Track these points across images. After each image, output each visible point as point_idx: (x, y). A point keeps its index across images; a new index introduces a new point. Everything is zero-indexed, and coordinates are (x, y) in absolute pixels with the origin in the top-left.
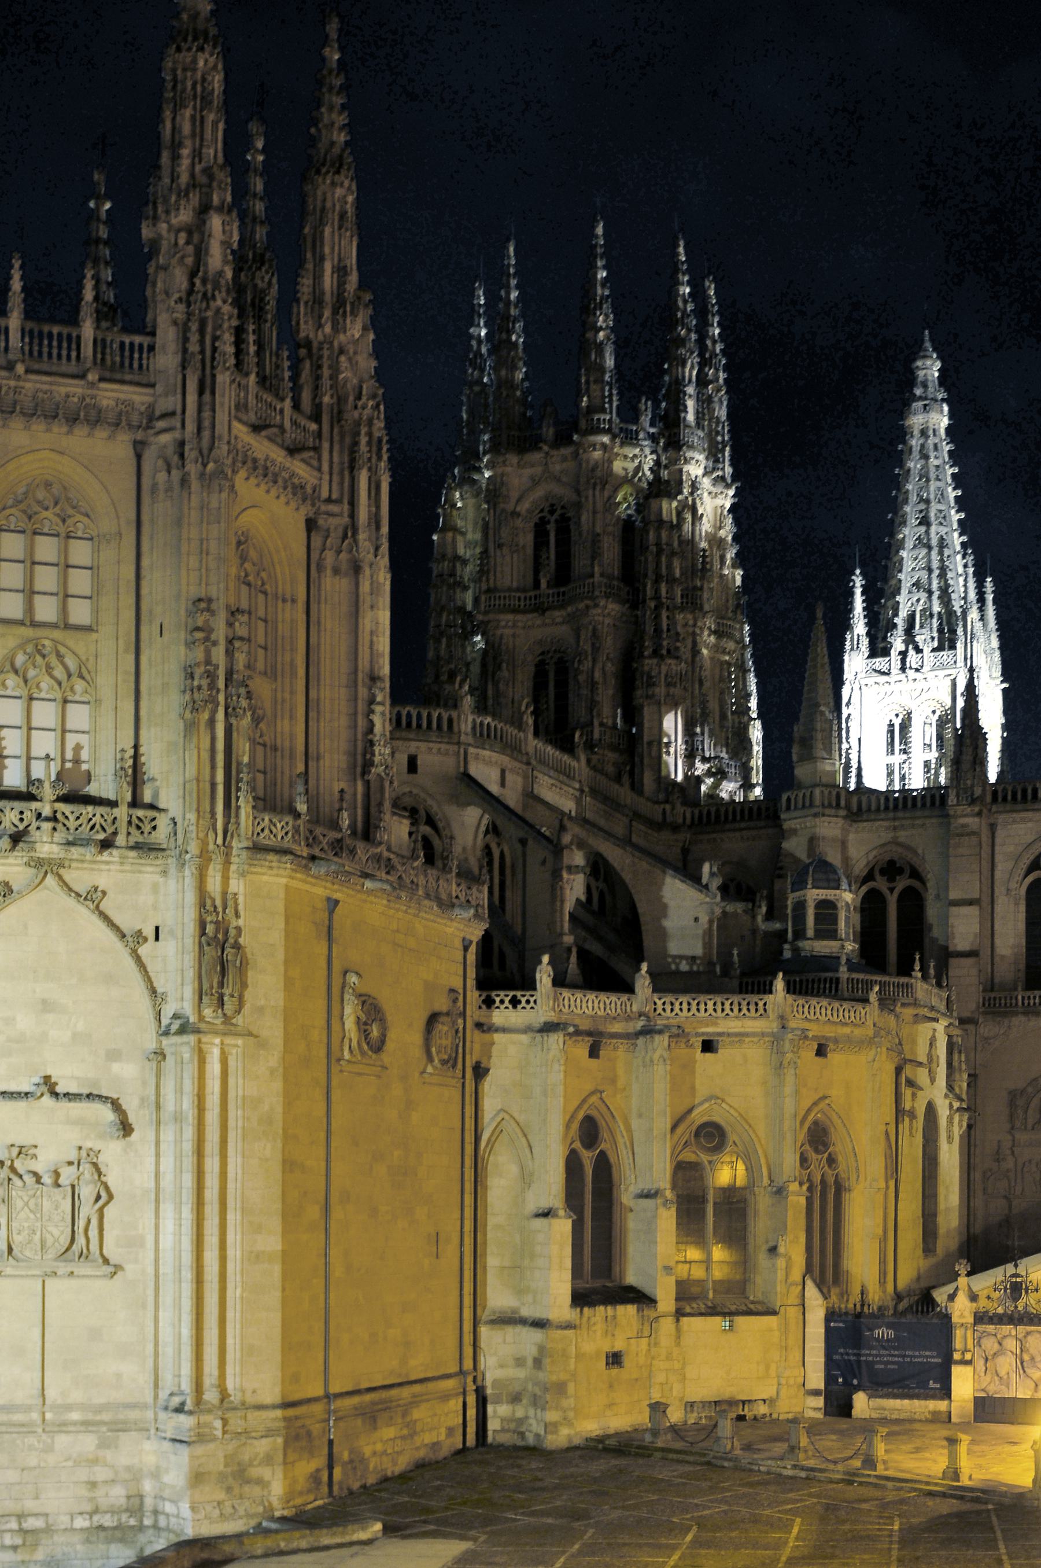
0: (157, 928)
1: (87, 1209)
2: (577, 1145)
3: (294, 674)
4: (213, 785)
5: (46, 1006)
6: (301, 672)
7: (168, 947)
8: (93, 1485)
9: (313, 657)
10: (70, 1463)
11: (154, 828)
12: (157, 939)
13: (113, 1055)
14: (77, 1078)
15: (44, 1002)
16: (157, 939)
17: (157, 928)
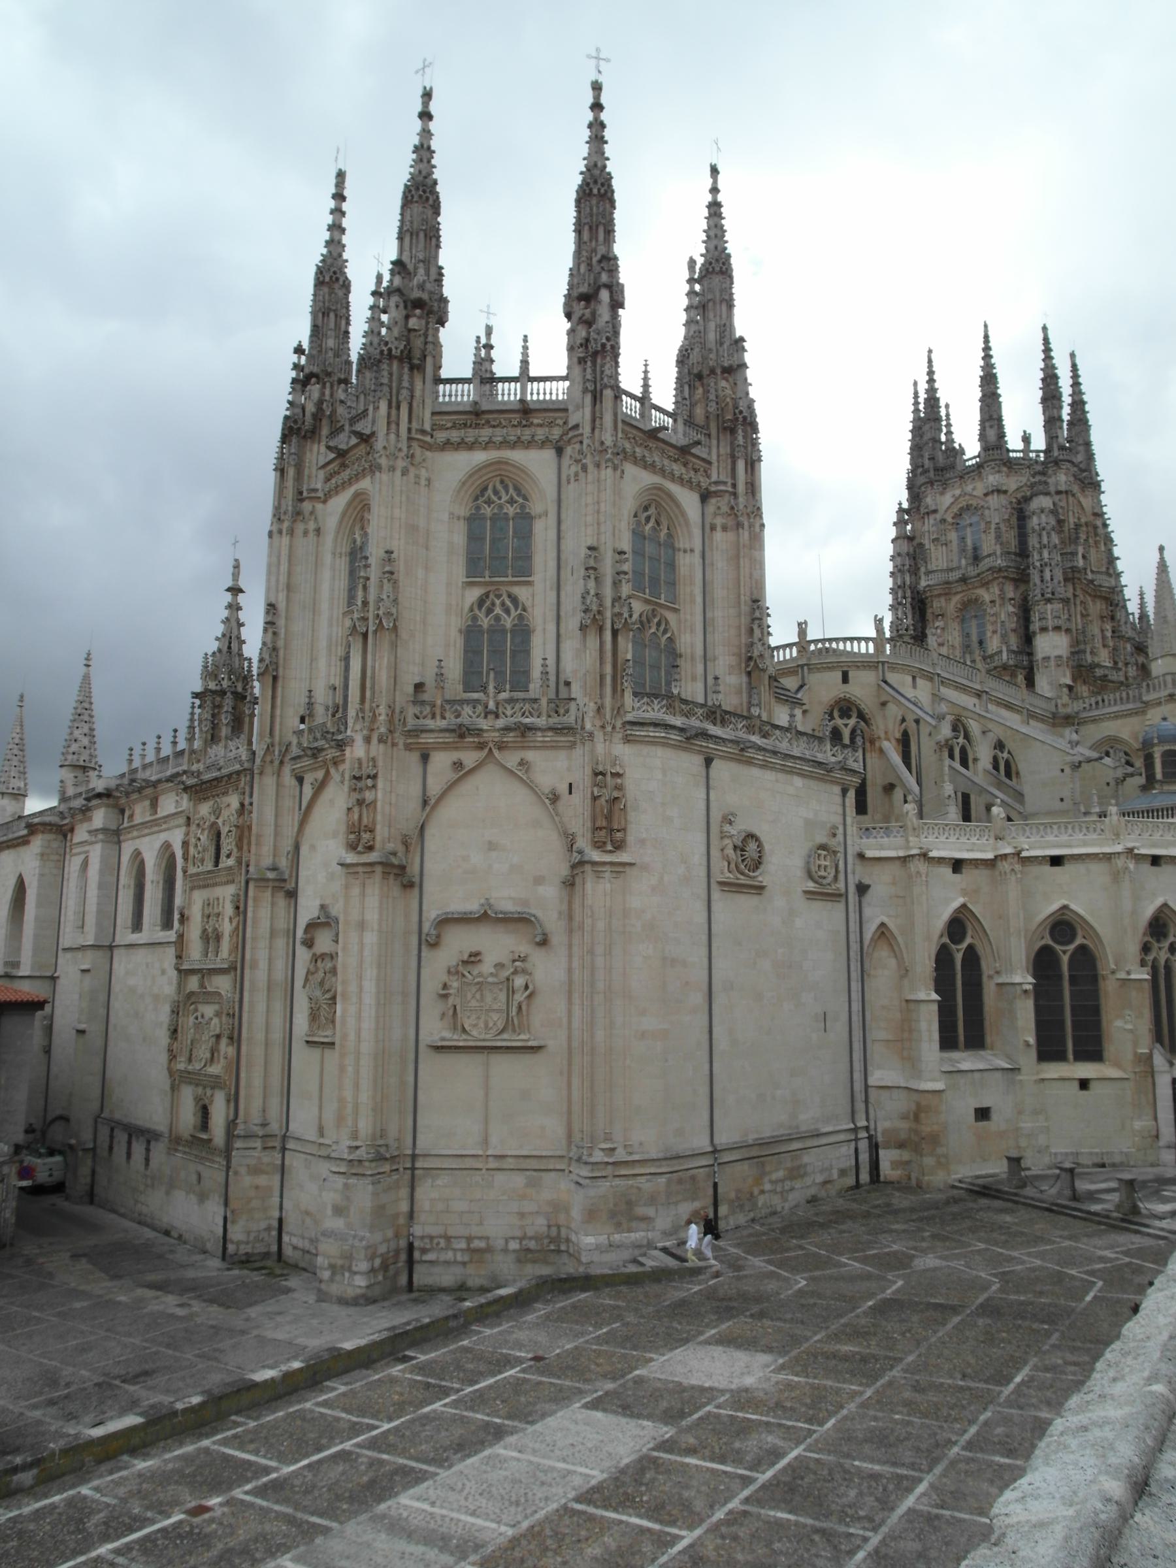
0: (570, 784)
1: (520, 997)
2: (946, 940)
3: (693, 601)
4: (602, 677)
5: (492, 846)
6: (699, 599)
7: (576, 798)
8: (522, 1215)
9: (707, 589)
10: (505, 1197)
11: (567, 711)
12: (570, 793)
13: (539, 880)
14: (510, 898)
15: (490, 843)
16: (570, 793)
17: (570, 784)
